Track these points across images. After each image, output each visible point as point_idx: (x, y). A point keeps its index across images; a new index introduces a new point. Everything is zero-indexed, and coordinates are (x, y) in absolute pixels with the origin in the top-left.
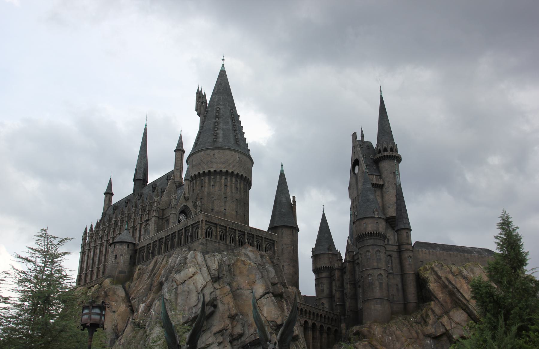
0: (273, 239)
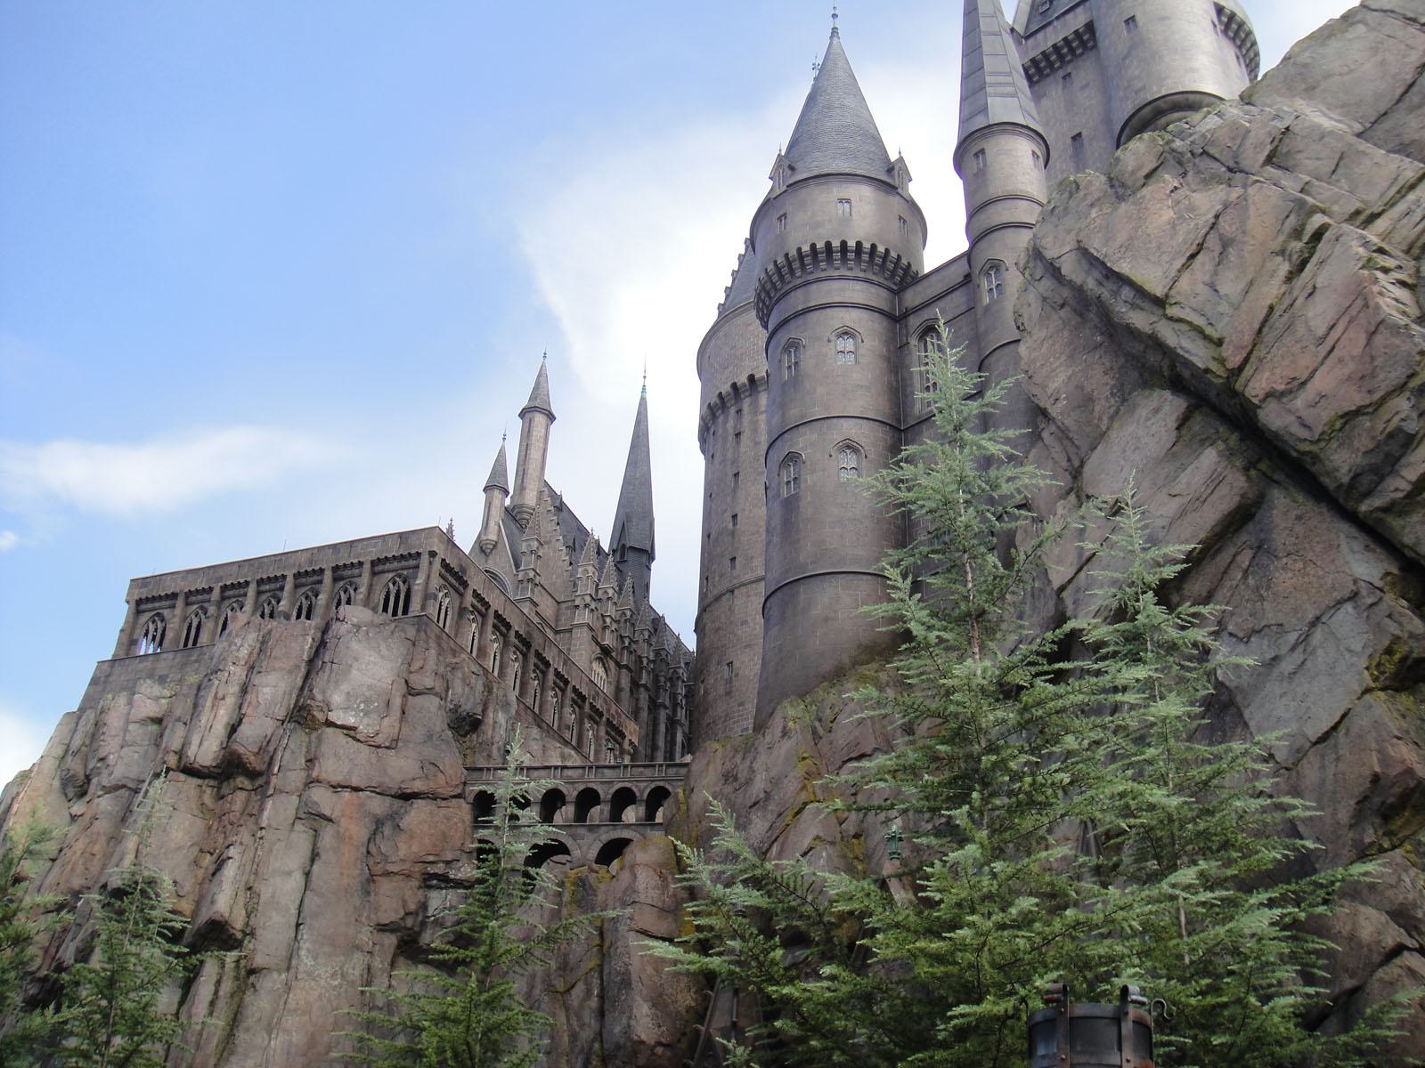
0: (413, 551)
